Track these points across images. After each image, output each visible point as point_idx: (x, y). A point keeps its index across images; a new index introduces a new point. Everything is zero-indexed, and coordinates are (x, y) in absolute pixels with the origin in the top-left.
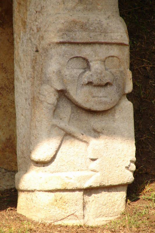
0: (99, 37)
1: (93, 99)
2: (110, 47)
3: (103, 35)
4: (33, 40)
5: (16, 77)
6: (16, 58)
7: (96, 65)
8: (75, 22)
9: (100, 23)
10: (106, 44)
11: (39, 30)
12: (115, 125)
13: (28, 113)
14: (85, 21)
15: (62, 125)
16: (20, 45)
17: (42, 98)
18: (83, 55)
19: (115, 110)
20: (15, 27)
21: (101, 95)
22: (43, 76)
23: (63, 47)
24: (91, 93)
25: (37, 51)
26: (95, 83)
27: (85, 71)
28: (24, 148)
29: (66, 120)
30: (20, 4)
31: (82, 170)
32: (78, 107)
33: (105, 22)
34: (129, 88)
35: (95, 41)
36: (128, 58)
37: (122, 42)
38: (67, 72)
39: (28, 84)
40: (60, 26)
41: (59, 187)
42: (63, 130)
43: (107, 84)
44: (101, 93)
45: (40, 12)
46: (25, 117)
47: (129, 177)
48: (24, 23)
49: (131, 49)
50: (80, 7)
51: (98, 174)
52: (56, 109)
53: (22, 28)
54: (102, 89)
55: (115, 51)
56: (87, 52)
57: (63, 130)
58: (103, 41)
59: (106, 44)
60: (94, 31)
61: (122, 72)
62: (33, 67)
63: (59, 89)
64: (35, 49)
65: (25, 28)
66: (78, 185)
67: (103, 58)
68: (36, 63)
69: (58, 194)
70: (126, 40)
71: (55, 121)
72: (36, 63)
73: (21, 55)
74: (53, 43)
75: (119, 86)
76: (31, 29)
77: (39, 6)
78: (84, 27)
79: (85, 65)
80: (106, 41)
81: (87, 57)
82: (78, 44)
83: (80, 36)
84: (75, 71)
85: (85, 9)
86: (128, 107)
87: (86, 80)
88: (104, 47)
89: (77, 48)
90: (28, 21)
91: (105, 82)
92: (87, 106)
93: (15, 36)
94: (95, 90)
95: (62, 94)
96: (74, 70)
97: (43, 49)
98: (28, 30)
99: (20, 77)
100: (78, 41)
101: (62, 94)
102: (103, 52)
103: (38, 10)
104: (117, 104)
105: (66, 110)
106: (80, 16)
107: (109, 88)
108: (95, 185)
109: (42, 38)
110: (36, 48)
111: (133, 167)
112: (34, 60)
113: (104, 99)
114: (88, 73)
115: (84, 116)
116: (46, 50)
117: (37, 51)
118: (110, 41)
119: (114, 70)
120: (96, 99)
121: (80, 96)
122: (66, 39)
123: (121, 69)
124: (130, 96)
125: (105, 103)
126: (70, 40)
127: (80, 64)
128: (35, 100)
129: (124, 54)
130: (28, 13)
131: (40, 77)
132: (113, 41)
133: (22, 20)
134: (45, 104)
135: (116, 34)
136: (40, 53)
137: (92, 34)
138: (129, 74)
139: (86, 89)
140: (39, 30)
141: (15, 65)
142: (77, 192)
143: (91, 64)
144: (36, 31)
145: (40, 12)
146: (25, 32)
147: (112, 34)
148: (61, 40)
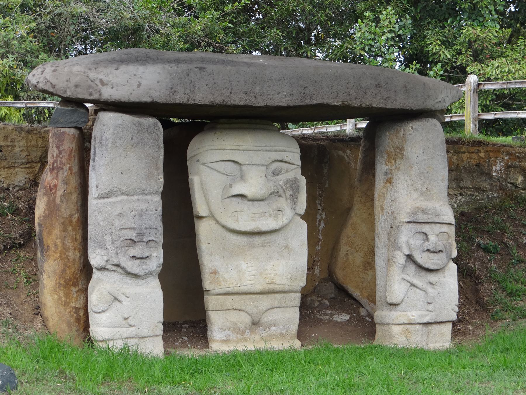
0: (435, 219)
1: (430, 261)
2: (441, 225)
3: (437, 217)
4: (388, 220)
5: (376, 245)
6: (376, 232)
7: (432, 238)
8: (418, 208)
9: (435, 209)
10: (439, 223)
11: (393, 213)
12: (445, 280)
13: (385, 270)
14: (425, 207)
15: (409, 278)
16: (379, 223)
17: (395, 260)
18: (424, 231)
19: (445, 269)
20: (376, 211)
21: (435, 258)
22: (396, 245)
23: (410, 225)
24: (429, 257)
25: (392, 228)
26: (432, 250)
27: (424, 243)
28: (382, 294)
29: (411, 276)
30: (379, 195)
31: (421, 310)
32: (420, 267)
33: (438, 208)
34: (455, 254)
35: (432, 221)
36: (454, 234)
37: (450, 222)
38: (412, 242)
39: (385, 251)
40: (409, 211)
41: (406, 322)
42: (409, 282)
43: (440, 251)
44: (435, 257)
45: (393, 201)
46: (382, 273)
47: (454, 317)
48: (383, 209)
49: (456, 228)
50: (422, 198)
51: (433, 313)
52: (404, 267)
53: (381, 212)
54: (436, 254)
55: (445, 228)
56: (426, 228)
57: (409, 282)
58: (437, 221)
59: (439, 223)
60: (431, 215)
61: (450, 243)
62: (389, 239)
63: (407, 254)
64: (390, 226)
65: (383, 212)
66: (419, 321)
67: (437, 233)
68: (390, 235)
69: (405, 326)
70: (453, 221)
71: (404, 276)
72: (390, 235)
73: (380, 230)
74: (403, 222)
75: (447, 253)
76: (387, 212)
77: (393, 197)
78: (424, 212)
79: (425, 238)
80: (439, 221)
81: (426, 233)
82: (420, 223)
83: (421, 218)
84: (418, 241)
85: (425, 199)
86: (453, 267)
87: (426, 249)
88: (438, 225)
89: (419, 226)
90: (385, 207)
91: (438, 250)
92: (426, 266)
93: (376, 217)
94: (432, 255)
95: (410, 257)
96: (417, 242)
97: (396, 226)
98: (385, 213)
99: (379, 245)
100: (420, 221)
101: (410, 257)
102: (438, 229)
103: (392, 199)
104: (446, 266)
105: (412, 268)
106: (422, 204)
107: (441, 254)
108: (430, 321)
109: (396, 218)
110: (391, 225)
111: (457, 309)
112: (390, 234)
113: (437, 261)
114: (427, 243)
115: (423, 273)
116: (398, 227)
117: (392, 228)
118: (442, 222)
119: (444, 242)
120: (432, 261)
121: (422, 258)
122: (411, 220)
123: (449, 241)
124: (455, 261)
125: (438, 264)
126: (415, 221)
127: (421, 237)
128: (389, 262)
129: (452, 231)
130: (385, 201)
131: (394, 246)
132: (444, 222)
133: (381, 206)
134: (397, 264)
135: (446, 217)
136: (393, 229)
137: (430, 217)
138: (455, 245)
139: (426, 254)
140: (393, 213)
141: (376, 238)
142: (418, 325)
143: (429, 237)
144: (391, 213)
145: (393, 201)
146: (383, 215)
147: (443, 217)
148: (409, 220)
